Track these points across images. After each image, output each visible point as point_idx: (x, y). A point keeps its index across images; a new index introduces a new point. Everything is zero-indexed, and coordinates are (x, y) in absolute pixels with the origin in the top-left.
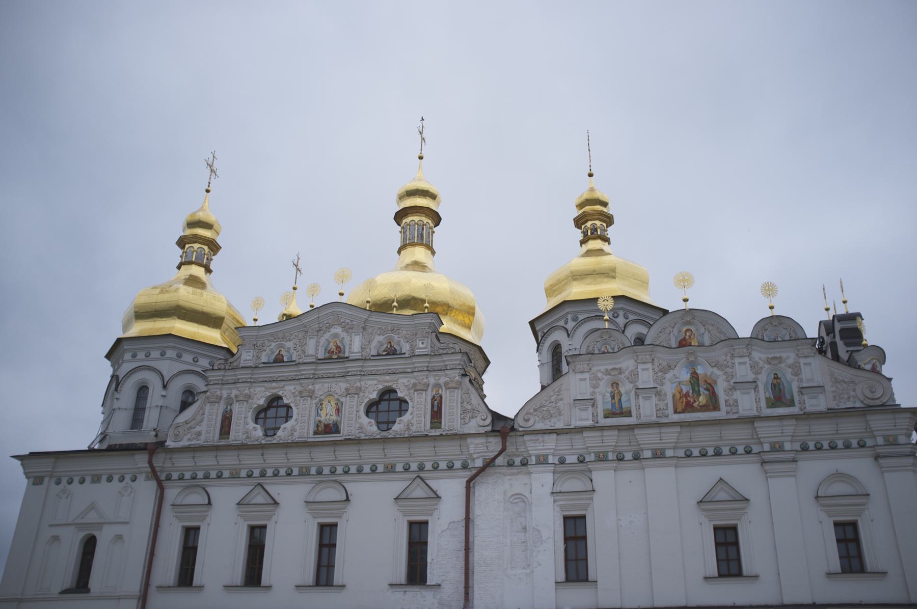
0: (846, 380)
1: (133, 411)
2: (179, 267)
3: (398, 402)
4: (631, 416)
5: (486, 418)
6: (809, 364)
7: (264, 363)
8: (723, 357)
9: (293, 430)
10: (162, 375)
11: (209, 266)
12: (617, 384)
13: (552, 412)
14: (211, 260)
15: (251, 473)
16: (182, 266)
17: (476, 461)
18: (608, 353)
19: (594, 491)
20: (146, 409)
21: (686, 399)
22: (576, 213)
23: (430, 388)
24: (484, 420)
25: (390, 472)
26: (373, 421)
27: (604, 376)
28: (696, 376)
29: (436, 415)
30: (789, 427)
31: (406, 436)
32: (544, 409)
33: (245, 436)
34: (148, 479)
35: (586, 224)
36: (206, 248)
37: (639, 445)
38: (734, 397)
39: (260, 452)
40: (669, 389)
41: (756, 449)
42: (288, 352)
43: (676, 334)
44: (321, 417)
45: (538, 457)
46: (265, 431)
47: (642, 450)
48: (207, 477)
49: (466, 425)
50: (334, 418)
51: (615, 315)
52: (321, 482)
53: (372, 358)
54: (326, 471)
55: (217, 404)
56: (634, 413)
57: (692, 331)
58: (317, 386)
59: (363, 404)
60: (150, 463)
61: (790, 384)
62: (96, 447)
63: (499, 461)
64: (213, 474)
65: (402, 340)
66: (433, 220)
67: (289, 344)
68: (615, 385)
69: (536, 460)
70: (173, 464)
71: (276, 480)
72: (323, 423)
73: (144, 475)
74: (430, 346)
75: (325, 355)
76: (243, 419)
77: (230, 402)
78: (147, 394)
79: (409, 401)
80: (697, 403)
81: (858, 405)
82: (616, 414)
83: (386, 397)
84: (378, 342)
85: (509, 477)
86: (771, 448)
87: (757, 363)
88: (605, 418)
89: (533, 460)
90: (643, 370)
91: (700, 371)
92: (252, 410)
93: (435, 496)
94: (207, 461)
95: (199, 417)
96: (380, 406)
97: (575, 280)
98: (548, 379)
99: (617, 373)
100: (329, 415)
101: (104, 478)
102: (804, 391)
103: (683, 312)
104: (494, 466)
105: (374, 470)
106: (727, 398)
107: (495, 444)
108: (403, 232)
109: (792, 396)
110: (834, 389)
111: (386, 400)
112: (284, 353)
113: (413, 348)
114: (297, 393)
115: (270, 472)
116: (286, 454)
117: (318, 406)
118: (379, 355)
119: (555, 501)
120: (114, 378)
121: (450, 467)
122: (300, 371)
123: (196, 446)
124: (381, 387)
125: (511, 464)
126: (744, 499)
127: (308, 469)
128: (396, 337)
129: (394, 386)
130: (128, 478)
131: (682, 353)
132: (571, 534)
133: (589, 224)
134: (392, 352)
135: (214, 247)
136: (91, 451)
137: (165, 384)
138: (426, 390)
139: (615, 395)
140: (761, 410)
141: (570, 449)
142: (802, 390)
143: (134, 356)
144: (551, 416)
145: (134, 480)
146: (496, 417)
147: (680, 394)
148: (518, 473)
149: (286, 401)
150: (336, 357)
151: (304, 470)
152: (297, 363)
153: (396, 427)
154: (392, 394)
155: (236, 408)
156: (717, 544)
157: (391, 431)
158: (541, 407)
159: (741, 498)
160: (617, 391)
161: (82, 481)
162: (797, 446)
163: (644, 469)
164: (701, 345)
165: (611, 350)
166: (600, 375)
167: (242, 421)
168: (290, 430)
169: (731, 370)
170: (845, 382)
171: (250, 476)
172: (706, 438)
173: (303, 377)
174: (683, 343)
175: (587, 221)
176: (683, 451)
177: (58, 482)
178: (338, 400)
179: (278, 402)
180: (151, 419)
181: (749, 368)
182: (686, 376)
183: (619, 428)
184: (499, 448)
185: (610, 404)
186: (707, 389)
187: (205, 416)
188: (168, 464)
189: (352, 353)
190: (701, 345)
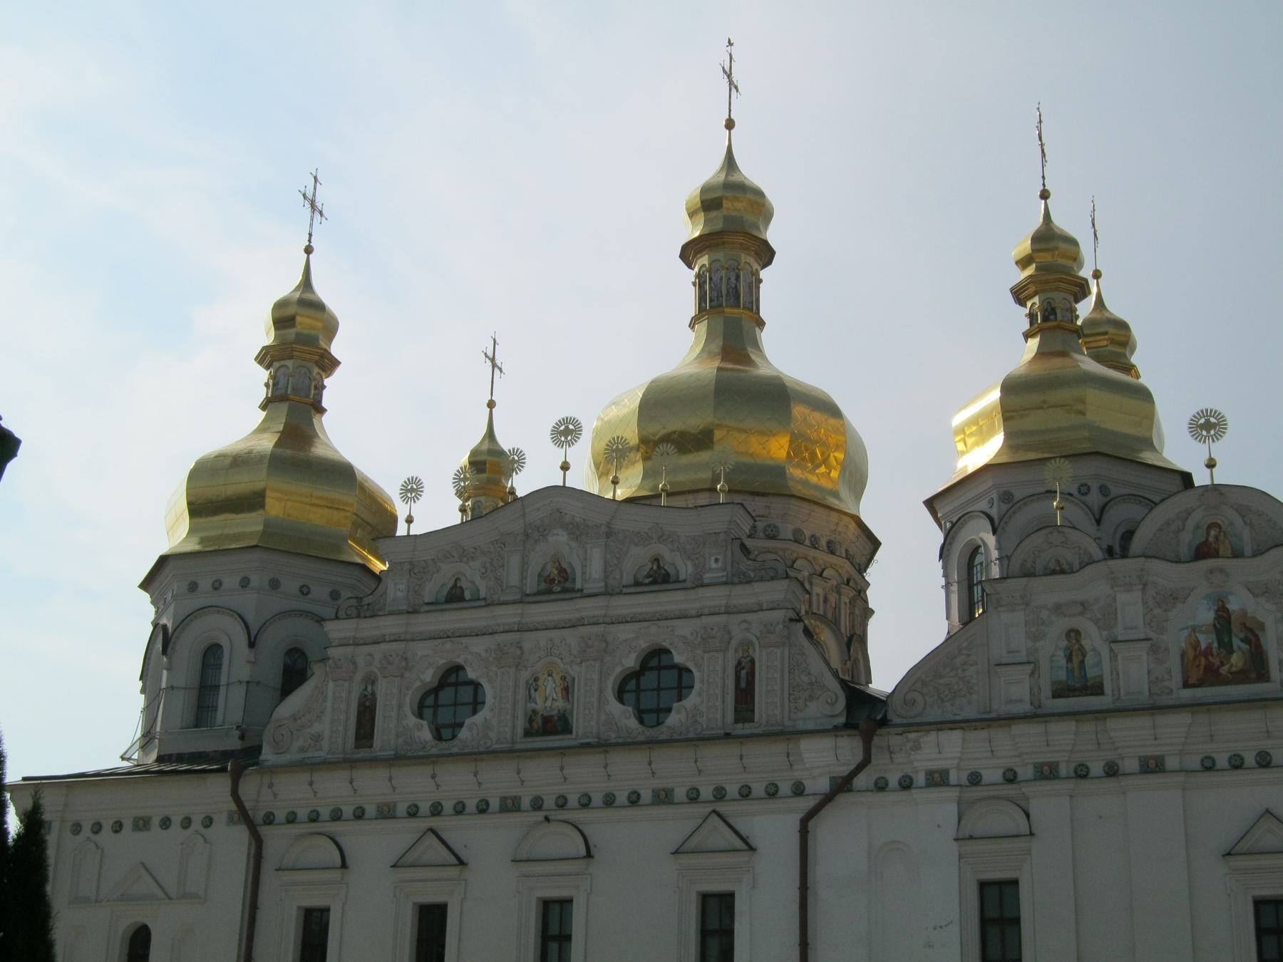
3: (674, 673)
5: (836, 701)
7: (428, 604)
11: (320, 401)
12: (1078, 633)
13: (956, 687)
15: (414, 809)
19: (1032, 834)
20: (221, 687)
24: (832, 704)
26: (630, 709)
29: (745, 697)
32: (942, 681)
33: (401, 740)
34: (231, 821)
39: (428, 770)
40: (1175, 641)
44: (536, 704)
45: (930, 774)
48: (337, 816)
50: (560, 704)
53: (625, 590)
56: (1108, 687)
59: (612, 678)
68: (1073, 634)
69: (927, 779)
72: (540, 715)
75: (538, 585)
77: (371, 680)
78: (221, 658)
79: (694, 670)
83: (654, 663)
84: (637, 559)
88: (1054, 697)
92: (410, 692)
93: (744, 846)
96: (642, 678)
104: (850, 790)
105: (634, 799)
107: (848, 750)
111: (651, 669)
112: (464, 584)
115: (448, 806)
117: (531, 682)
118: (637, 584)
121: (772, 792)
124: (643, 644)
125: (881, 786)
129: (666, 644)
130: (197, 825)
134: (660, 578)
137: (252, 639)
139: (1074, 653)
145: (208, 822)
147: (1196, 651)
149: (471, 674)
150: (559, 589)
151: (509, 802)
152: (489, 602)
153: (673, 719)
154: (664, 657)
155: (383, 690)
157: (663, 728)
160: (1076, 647)
161: (118, 827)
163: (1124, 793)
165: (1065, 567)
166: (1045, 614)
167: (394, 714)
173: (501, 629)
176: (1198, 758)
179: (457, 676)
180: (230, 705)
184: (859, 758)
187: (329, 704)
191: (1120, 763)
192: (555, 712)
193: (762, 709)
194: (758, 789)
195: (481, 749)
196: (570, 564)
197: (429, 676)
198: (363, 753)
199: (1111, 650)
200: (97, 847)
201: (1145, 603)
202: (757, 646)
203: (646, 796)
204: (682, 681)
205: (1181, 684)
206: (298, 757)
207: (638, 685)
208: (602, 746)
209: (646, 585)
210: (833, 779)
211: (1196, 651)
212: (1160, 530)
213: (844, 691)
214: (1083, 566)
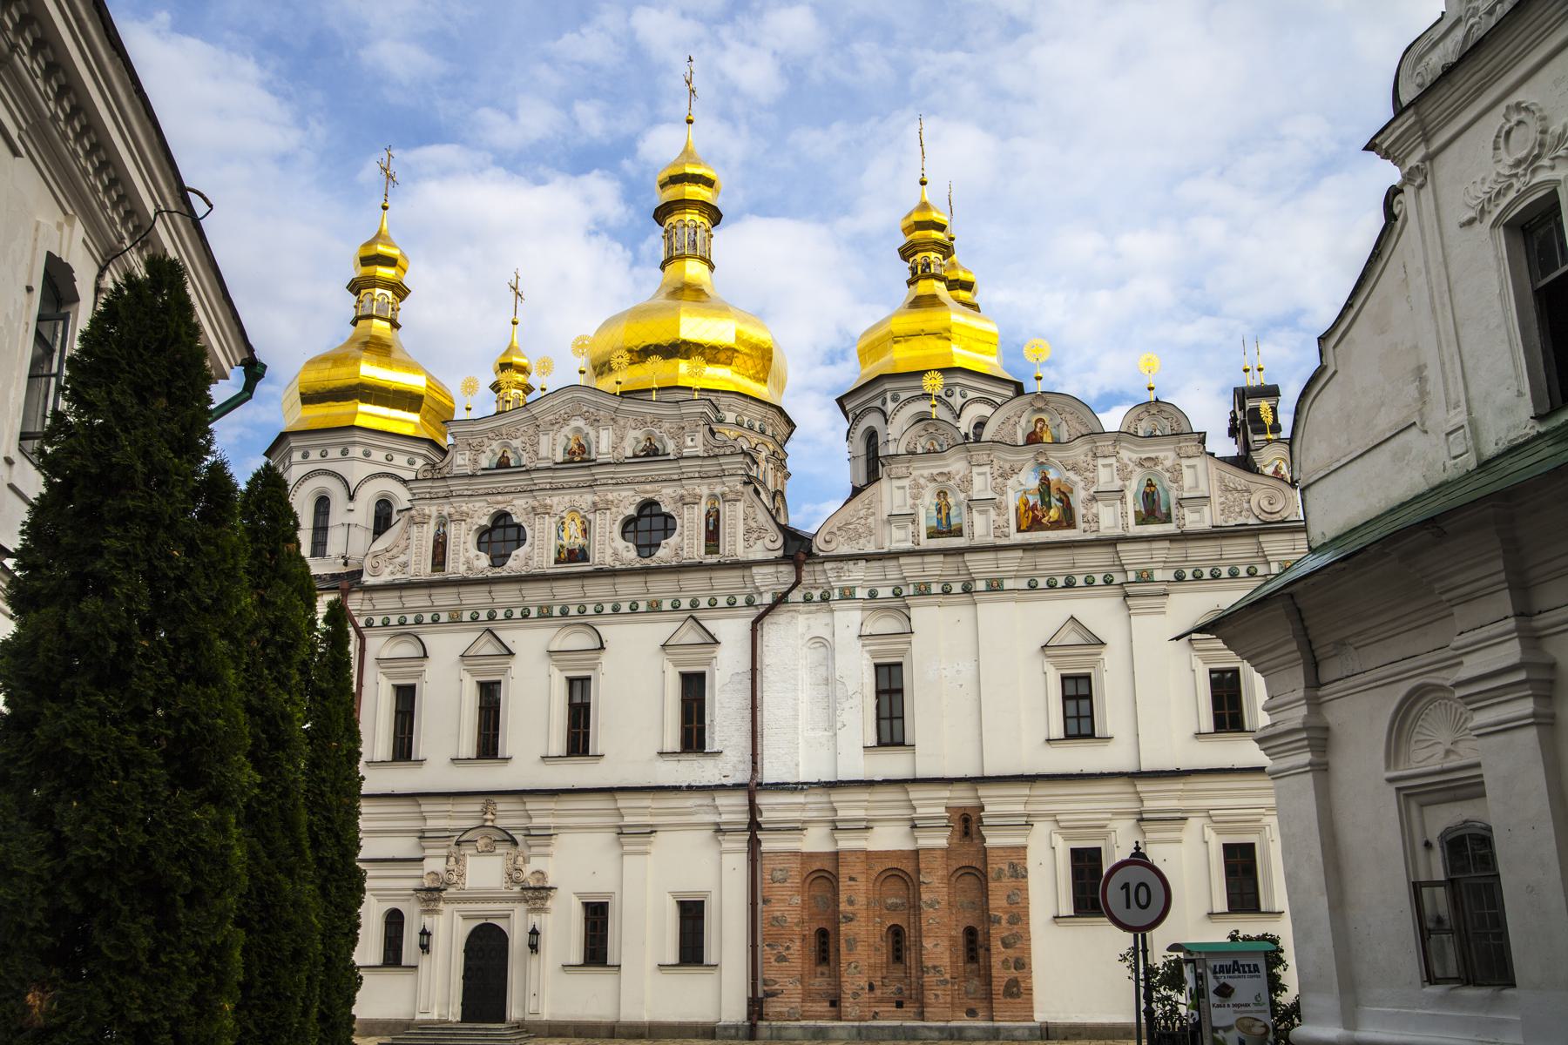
0: (1239, 488)
1: (311, 531)
2: (354, 323)
6: (1193, 467)
7: (483, 469)
8: (1082, 457)
9: (529, 558)
10: (346, 482)
12: (945, 493)
14: (399, 309)
16: (359, 322)
17: (764, 594)
18: (935, 452)
19: (912, 633)
22: (903, 240)
23: (704, 501)
26: (631, 545)
27: (929, 484)
29: (713, 537)
30: (1161, 550)
31: (674, 563)
35: (915, 257)
36: (389, 293)
38: (1094, 511)
39: (486, 588)
40: (1012, 500)
41: (1118, 578)
42: (515, 453)
43: (1024, 426)
45: (842, 589)
46: (491, 559)
47: (974, 580)
49: (751, 549)
50: (581, 541)
51: (949, 393)
54: (573, 611)
56: (966, 531)
58: (556, 500)
59: (618, 523)
61: (1166, 492)
63: (791, 597)
64: (427, 618)
65: (666, 437)
66: (710, 217)
67: (516, 443)
70: (374, 606)
71: (508, 624)
76: (462, 546)
80: (1047, 518)
81: (1252, 521)
83: (647, 511)
84: (632, 441)
85: (806, 616)
86: (1137, 577)
87: (1126, 466)
88: (928, 538)
89: (836, 594)
90: (979, 474)
91: (1052, 475)
94: (417, 600)
95: (403, 544)
97: (896, 342)
98: (862, 481)
99: (945, 479)
100: (573, 538)
103: (1033, 395)
104: (787, 602)
105: (634, 609)
106: (1084, 512)
107: (786, 573)
108: (668, 236)
109: (1169, 509)
110: (1223, 499)
112: (509, 454)
113: (679, 447)
114: (530, 509)
115: (500, 614)
116: (520, 590)
118: (635, 456)
119: (863, 646)
121: (731, 604)
122: (532, 479)
123: (403, 581)
124: (639, 499)
125: (808, 600)
127: (550, 608)
128: (657, 431)
129: (657, 498)
131: (1029, 454)
133: (919, 257)
135: (400, 291)
141: (883, 580)
142: (1180, 502)
143: (305, 456)
148: (818, 611)
149: (516, 520)
150: (578, 459)
154: (654, 507)
155: (452, 530)
157: (654, 558)
162: (1170, 575)
164: (1056, 442)
165: (938, 448)
166: (922, 481)
169: (1091, 475)
170: (1238, 491)
171: (474, 619)
172: (1053, 563)
174: (1033, 439)
175: (916, 253)
178: (584, 517)
181: (1115, 473)
182: (1033, 483)
183: (945, 552)
184: (793, 580)
186: (1060, 500)
188: (367, 606)
189: (600, 454)
190: (1056, 442)
192: (577, 547)
199: (969, 506)
203: (643, 607)
204: (667, 524)
207: (636, 526)
210: (773, 594)
211: (1025, 505)
213: (781, 531)
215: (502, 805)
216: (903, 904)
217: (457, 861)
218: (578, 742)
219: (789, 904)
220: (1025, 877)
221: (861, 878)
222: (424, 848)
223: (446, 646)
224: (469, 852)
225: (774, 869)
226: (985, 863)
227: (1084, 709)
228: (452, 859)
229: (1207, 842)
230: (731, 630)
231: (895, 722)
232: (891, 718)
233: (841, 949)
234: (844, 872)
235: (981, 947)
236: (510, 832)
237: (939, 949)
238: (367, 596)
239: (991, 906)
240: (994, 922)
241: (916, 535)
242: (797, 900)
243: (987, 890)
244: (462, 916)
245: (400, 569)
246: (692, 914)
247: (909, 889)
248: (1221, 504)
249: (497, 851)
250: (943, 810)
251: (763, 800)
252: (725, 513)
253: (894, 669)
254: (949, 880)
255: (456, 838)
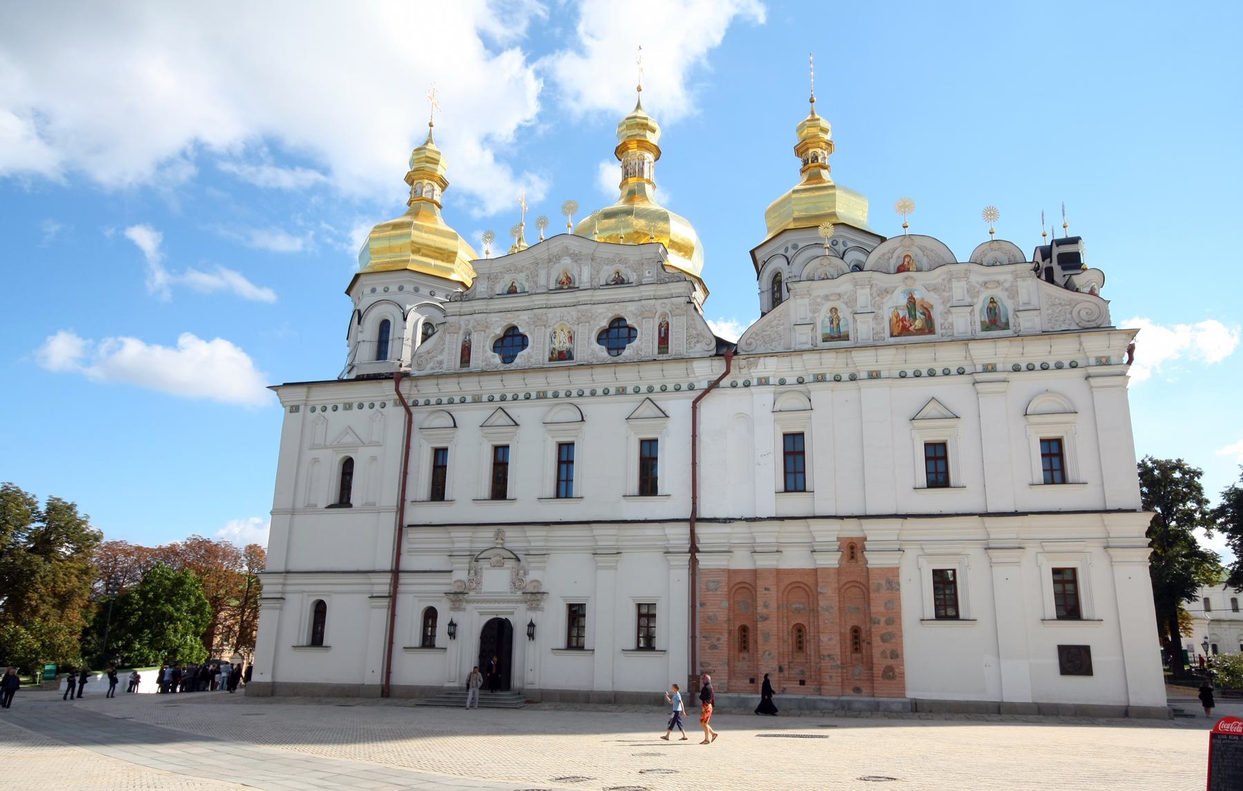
0: (1063, 302)
1: (377, 343)
3: (627, 329)
4: (848, 340)
12: (836, 309)
19: (812, 409)
21: (902, 322)
23: (657, 317)
24: (709, 345)
25: (621, 394)
27: (823, 302)
28: (913, 301)
29: (664, 341)
32: (765, 333)
33: (484, 364)
34: (396, 405)
37: (856, 367)
38: (950, 320)
39: (499, 377)
40: (887, 314)
48: (451, 402)
49: (691, 350)
50: (568, 345)
52: (558, 404)
54: (562, 394)
55: (456, 335)
56: (851, 337)
57: (910, 257)
59: (595, 332)
60: (397, 390)
62: (345, 378)
63: (722, 383)
64: (457, 399)
73: (392, 401)
74: (656, 276)
80: (913, 327)
82: (835, 338)
83: (616, 325)
84: (607, 273)
88: (823, 341)
91: (917, 296)
92: (489, 340)
94: (450, 388)
96: (610, 333)
101: (355, 406)
102: (1018, 313)
104: (718, 387)
105: (606, 392)
107: (719, 366)
112: (516, 284)
115: (509, 397)
118: (607, 284)
120: (357, 313)
121: (678, 389)
125: (734, 386)
126: (950, 414)
132: (790, 449)
134: (619, 281)
136: (340, 381)
138: (653, 318)
140: (975, 333)
143: (373, 290)
144: (772, 341)
145: (383, 406)
146: (720, 343)
149: (521, 330)
150: (567, 287)
151: (542, 394)
155: (475, 339)
156: (927, 459)
157: (620, 356)
158: (762, 331)
159: (951, 415)
160: (835, 316)
161: (335, 408)
165: (829, 276)
166: (819, 300)
168: (526, 358)
171: (491, 400)
172: (919, 358)
176: (898, 372)
177: (313, 410)
182: (903, 301)
185: (829, 329)
186: (923, 314)
187: (446, 346)
191: (857, 374)
192: (565, 349)
193: (675, 345)
194: (670, 387)
195: (526, 368)
196: (572, 274)
197: (499, 331)
198: (464, 370)
199: (854, 317)
200: (324, 418)
201: (871, 294)
202: (670, 316)
203: (612, 391)
204: (631, 334)
205: (889, 335)
206: (430, 372)
207: (608, 335)
208: (590, 365)
209: (611, 285)
211: (897, 318)
212: (880, 258)
214: (839, 276)
215: (510, 532)
216: (804, 609)
217: (476, 574)
218: (564, 487)
219: (718, 607)
220: (899, 590)
221: (773, 589)
222: (453, 564)
223: (470, 417)
224: (484, 566)
225: (708, 581)
226: (868, 581)
227: (941, 468)
228: (472, 572)
229: (1040, 567)
230: (678, 407)
231: (798, 475)
232: (795, 473)
233: (758, 641)
234: (760, 584)
235: (864, 641)
236: (515, 553)
237: (833, 642)
238: (414, 383)
239: (872, 611)
240: (874, 623)
241: (814, 339)
242: (725, 604)
243: (869, 599)
244: (479, 612)
245: (438, 365)
246: (646, 616)
247: (809, 598)
248: (1048, 315)
249: (505, 566)
250: (836, 539)
251: (701, 529)
252: (672, 325)
253: (797, 439)
254: (839, 591)
255: (475, 556)
